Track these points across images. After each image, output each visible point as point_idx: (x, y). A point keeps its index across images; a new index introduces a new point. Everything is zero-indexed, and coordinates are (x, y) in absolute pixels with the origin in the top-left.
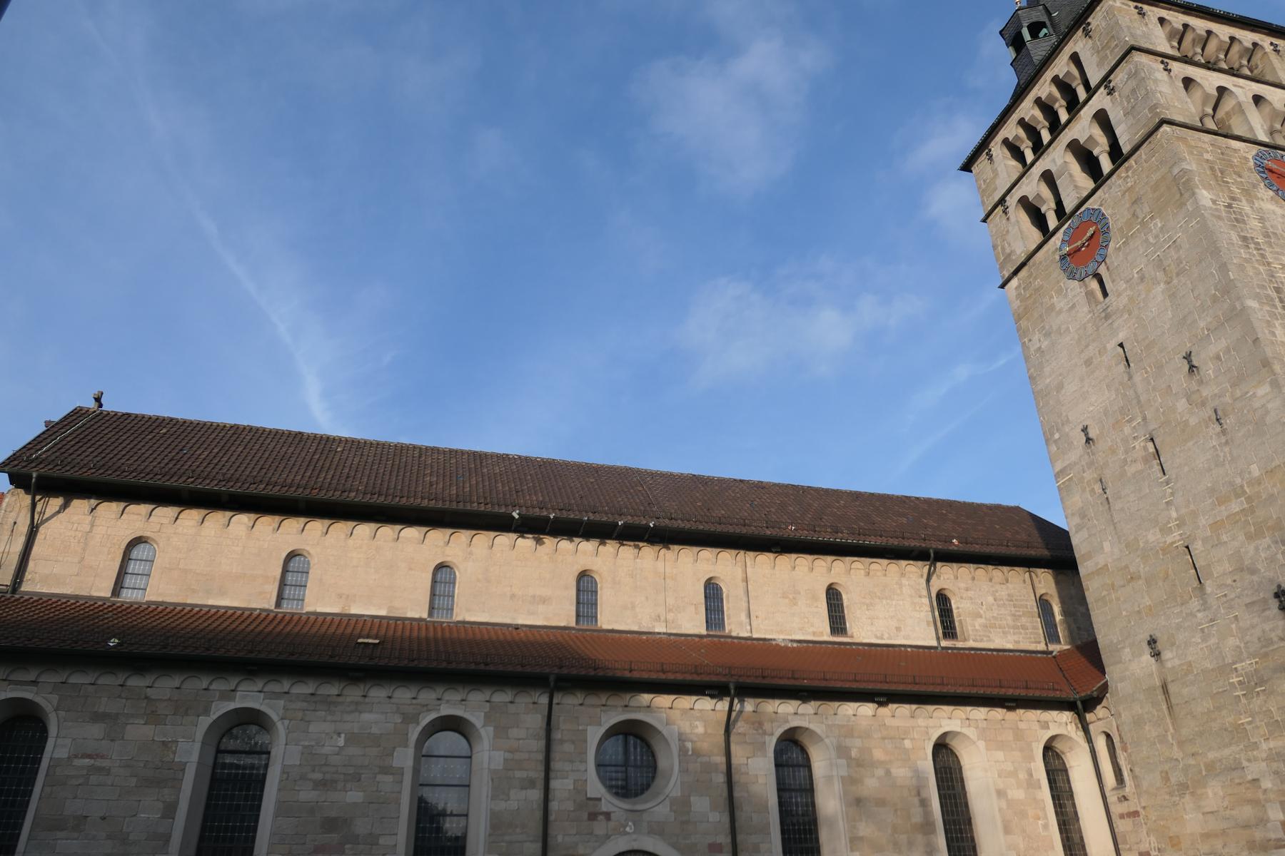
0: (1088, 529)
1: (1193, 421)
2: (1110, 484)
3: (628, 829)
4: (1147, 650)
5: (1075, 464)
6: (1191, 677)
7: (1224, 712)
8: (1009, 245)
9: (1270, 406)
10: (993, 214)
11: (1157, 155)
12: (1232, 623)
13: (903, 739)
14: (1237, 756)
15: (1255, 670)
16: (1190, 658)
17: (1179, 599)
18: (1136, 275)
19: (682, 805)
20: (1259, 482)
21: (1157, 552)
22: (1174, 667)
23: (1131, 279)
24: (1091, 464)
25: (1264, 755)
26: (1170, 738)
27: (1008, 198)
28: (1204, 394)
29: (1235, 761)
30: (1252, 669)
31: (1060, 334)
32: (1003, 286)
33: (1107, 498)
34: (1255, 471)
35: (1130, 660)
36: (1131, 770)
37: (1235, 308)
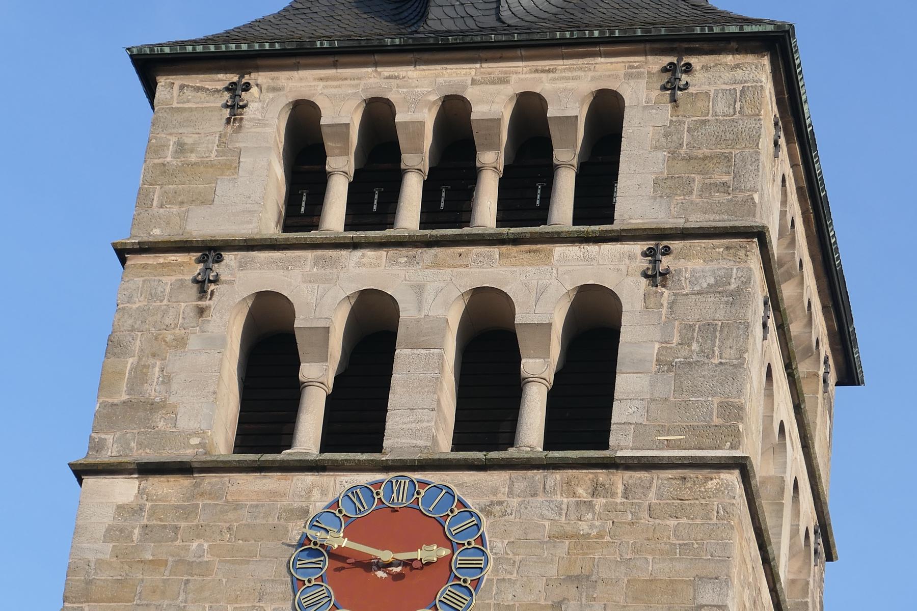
8: (167, 380)
10: (162, 259)
27: (229, 257)
32: (81, 472)
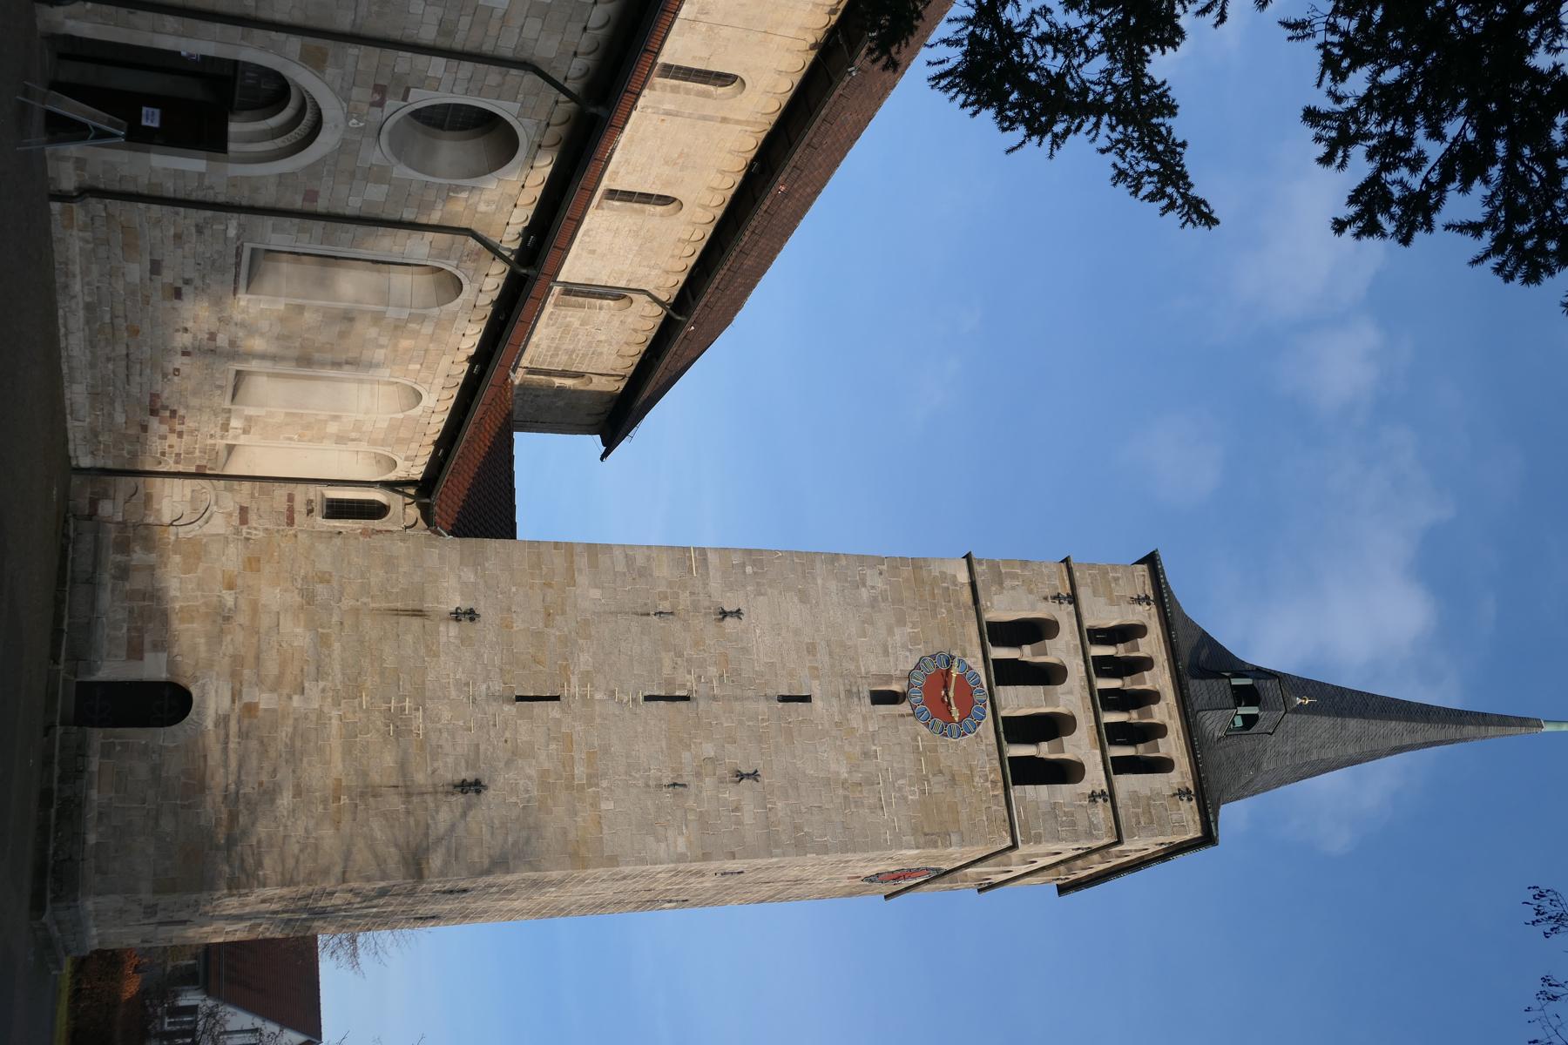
0: (624, 573)
1: (686, 756)
2: (662, 624)
4: (465, 606)
5: (705, 585)
6: (423, 651)
7: (377, 679)
8: (1013, 588)
9: (663, 845)
10: (1066, 578)
11: (986, 823)
12: (464, 723)
14: (330, 678)
15: (412, 731)
16: (443, 658)
17: (508, 667)
18: (874, 748)
20: (595, 805)
21: (566, 659)
23: (873, 740)
26: (365, 600)
27: (1071, 607)
28: (707, 779)
29: (326, 673)
30: (413, 728)
31: (864, 622)
32: (968, 557)
33: (648, 614)
34: (606, 806)
35: (460, 577)
36: (340, 533)
37: (777, 846)
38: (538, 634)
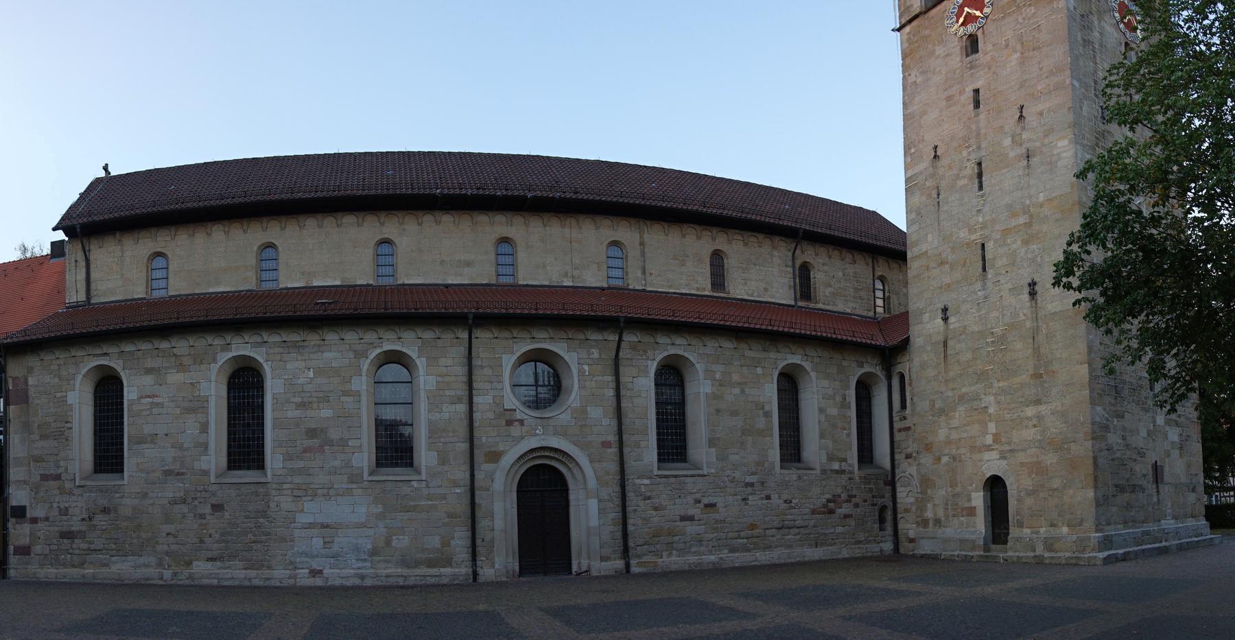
3: (538, 431)
4: (940, 314)
13: (756, 367)
19: (581, 413)
22: (954, 328)
24: (933, 175)
25: (994, 391)
38: (952, 268)
